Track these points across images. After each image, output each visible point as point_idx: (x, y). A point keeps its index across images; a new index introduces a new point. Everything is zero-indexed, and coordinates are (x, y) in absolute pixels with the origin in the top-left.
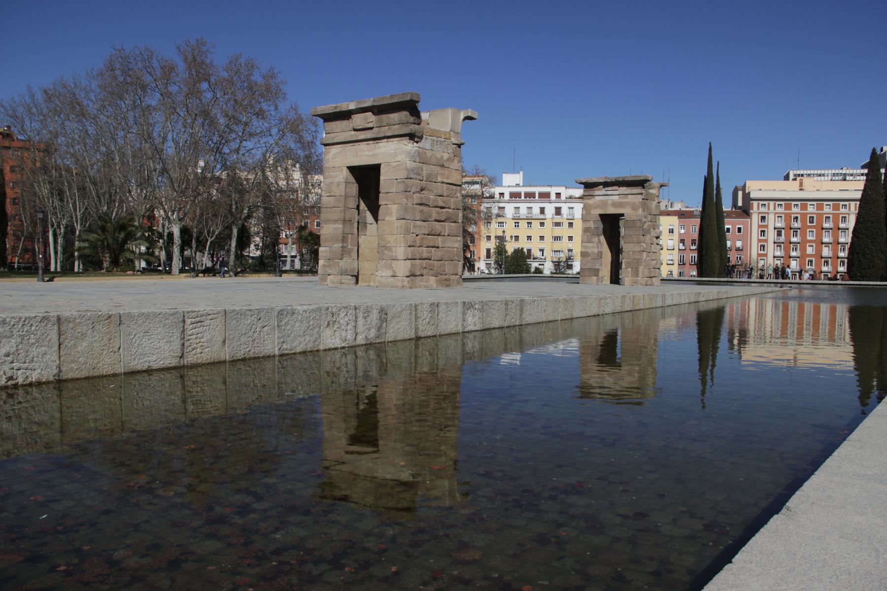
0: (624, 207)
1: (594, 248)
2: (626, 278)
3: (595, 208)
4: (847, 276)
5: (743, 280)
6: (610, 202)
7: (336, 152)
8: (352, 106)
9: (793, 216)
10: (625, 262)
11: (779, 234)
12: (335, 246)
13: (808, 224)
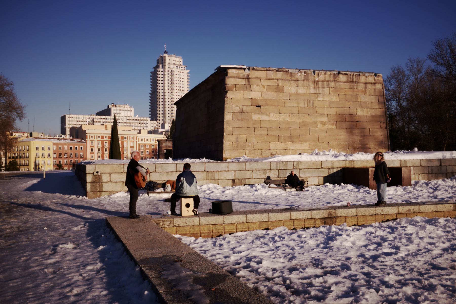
9: (105, 142)
11: (99, 150)
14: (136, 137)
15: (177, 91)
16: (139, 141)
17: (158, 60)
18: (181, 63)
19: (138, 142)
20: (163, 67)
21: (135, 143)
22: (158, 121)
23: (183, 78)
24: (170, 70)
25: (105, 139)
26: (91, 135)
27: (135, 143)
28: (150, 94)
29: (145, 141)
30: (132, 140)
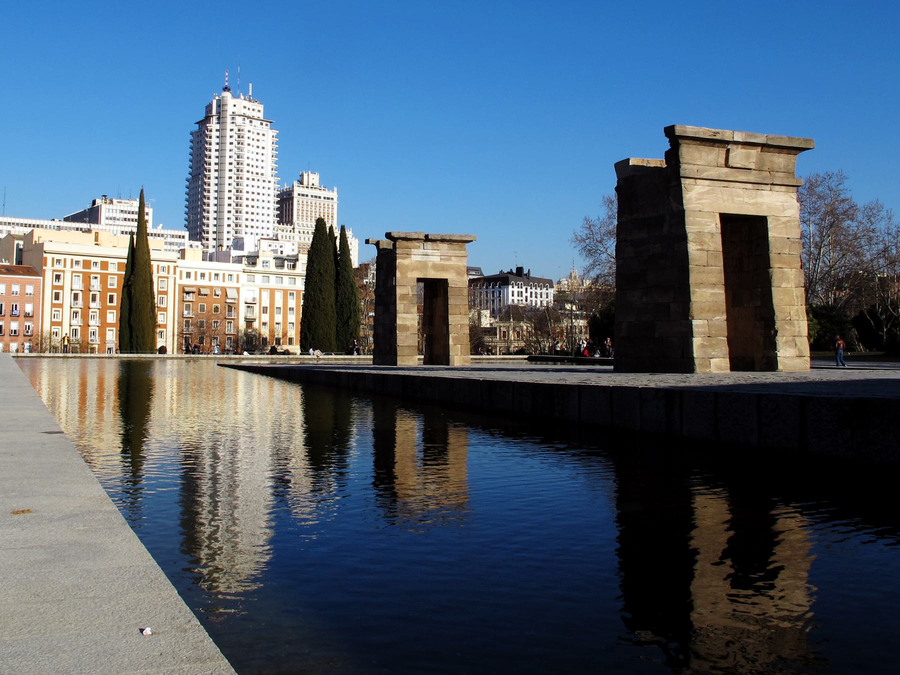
0: (447, 271)
1: (413, 319)
2: (456, 357)
3: (413, 270)
4: (119, 351)
5: (57, 355)
6: (430, 264)
7: (700, 191)
8: (738, 137)
10: (454, 339)
11: (76, 297)
12: (717, 318)
13: (109, 287)
14: (175, 267)
15: (249, 175)
16: (181, 278)
17: (209, 108)
18: (261, 115)
19: (178, 282)
20: (220, 119)
21: (171, 281)
22: (204, 242)
23: (263, 148)
24: (236, 129)
25: (94, 269)
26: (57, 257)
27: (171, 281)
28: (187, 180)
29: (196, 279)
30: (165, 274)
